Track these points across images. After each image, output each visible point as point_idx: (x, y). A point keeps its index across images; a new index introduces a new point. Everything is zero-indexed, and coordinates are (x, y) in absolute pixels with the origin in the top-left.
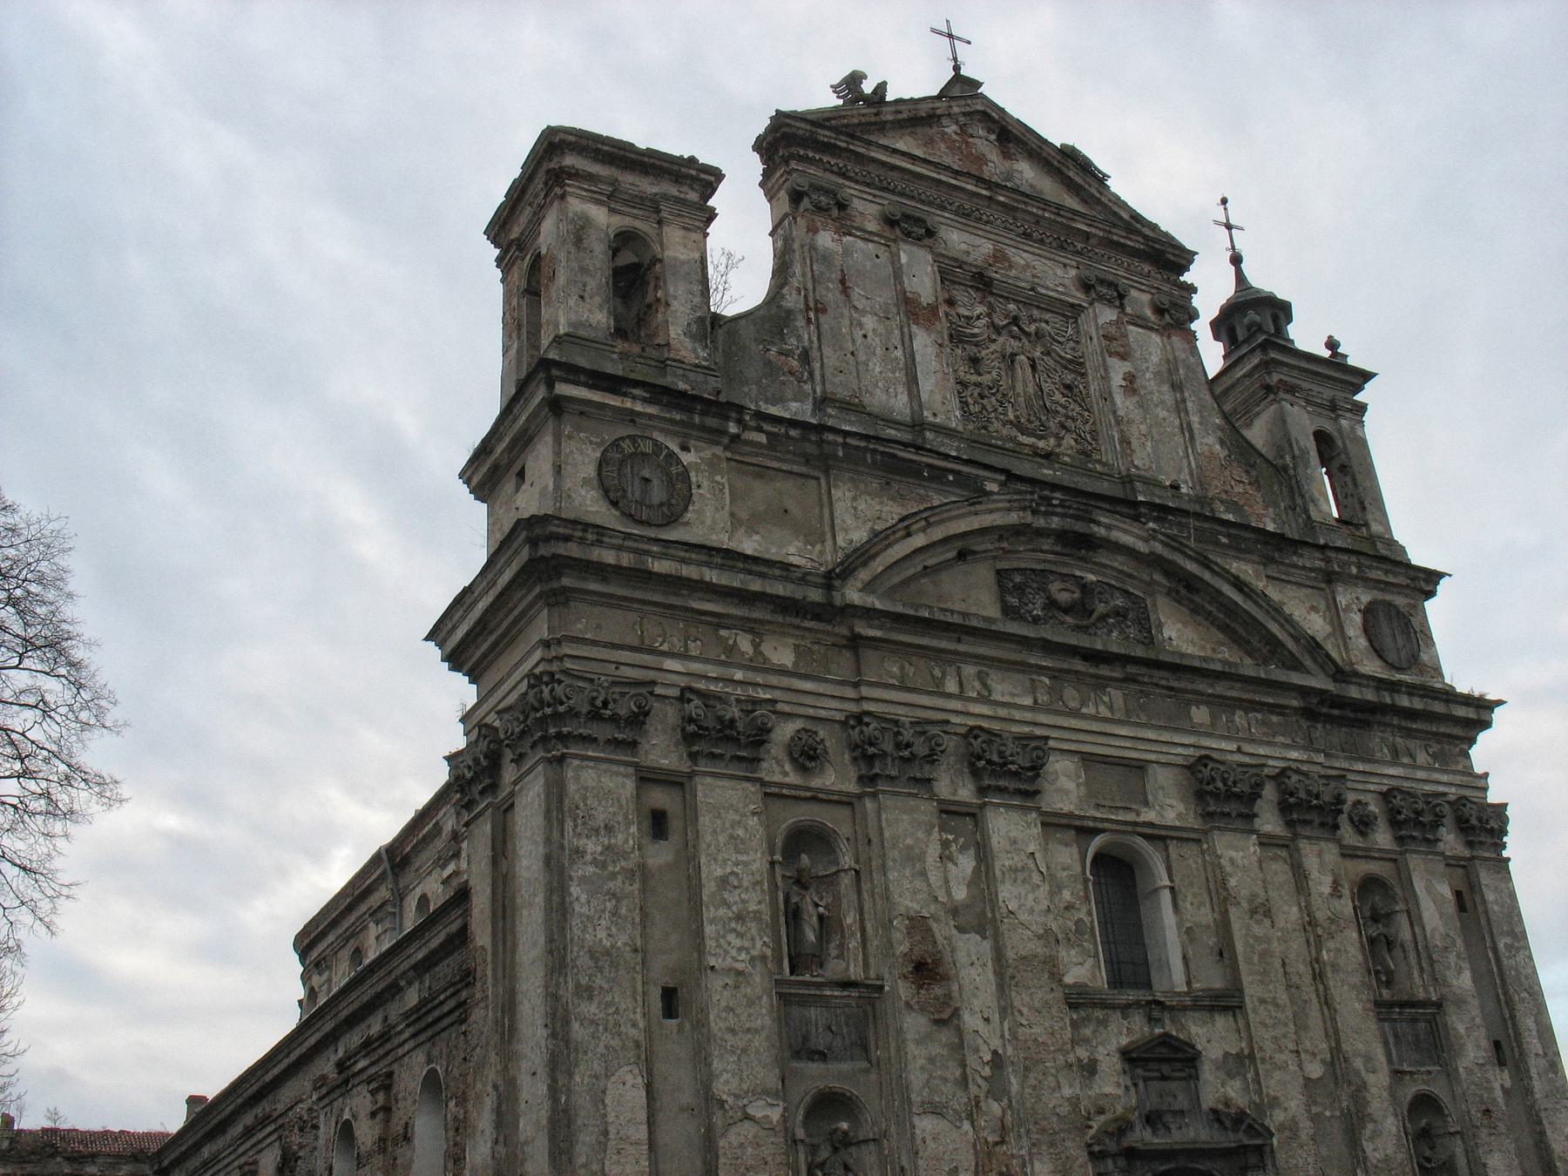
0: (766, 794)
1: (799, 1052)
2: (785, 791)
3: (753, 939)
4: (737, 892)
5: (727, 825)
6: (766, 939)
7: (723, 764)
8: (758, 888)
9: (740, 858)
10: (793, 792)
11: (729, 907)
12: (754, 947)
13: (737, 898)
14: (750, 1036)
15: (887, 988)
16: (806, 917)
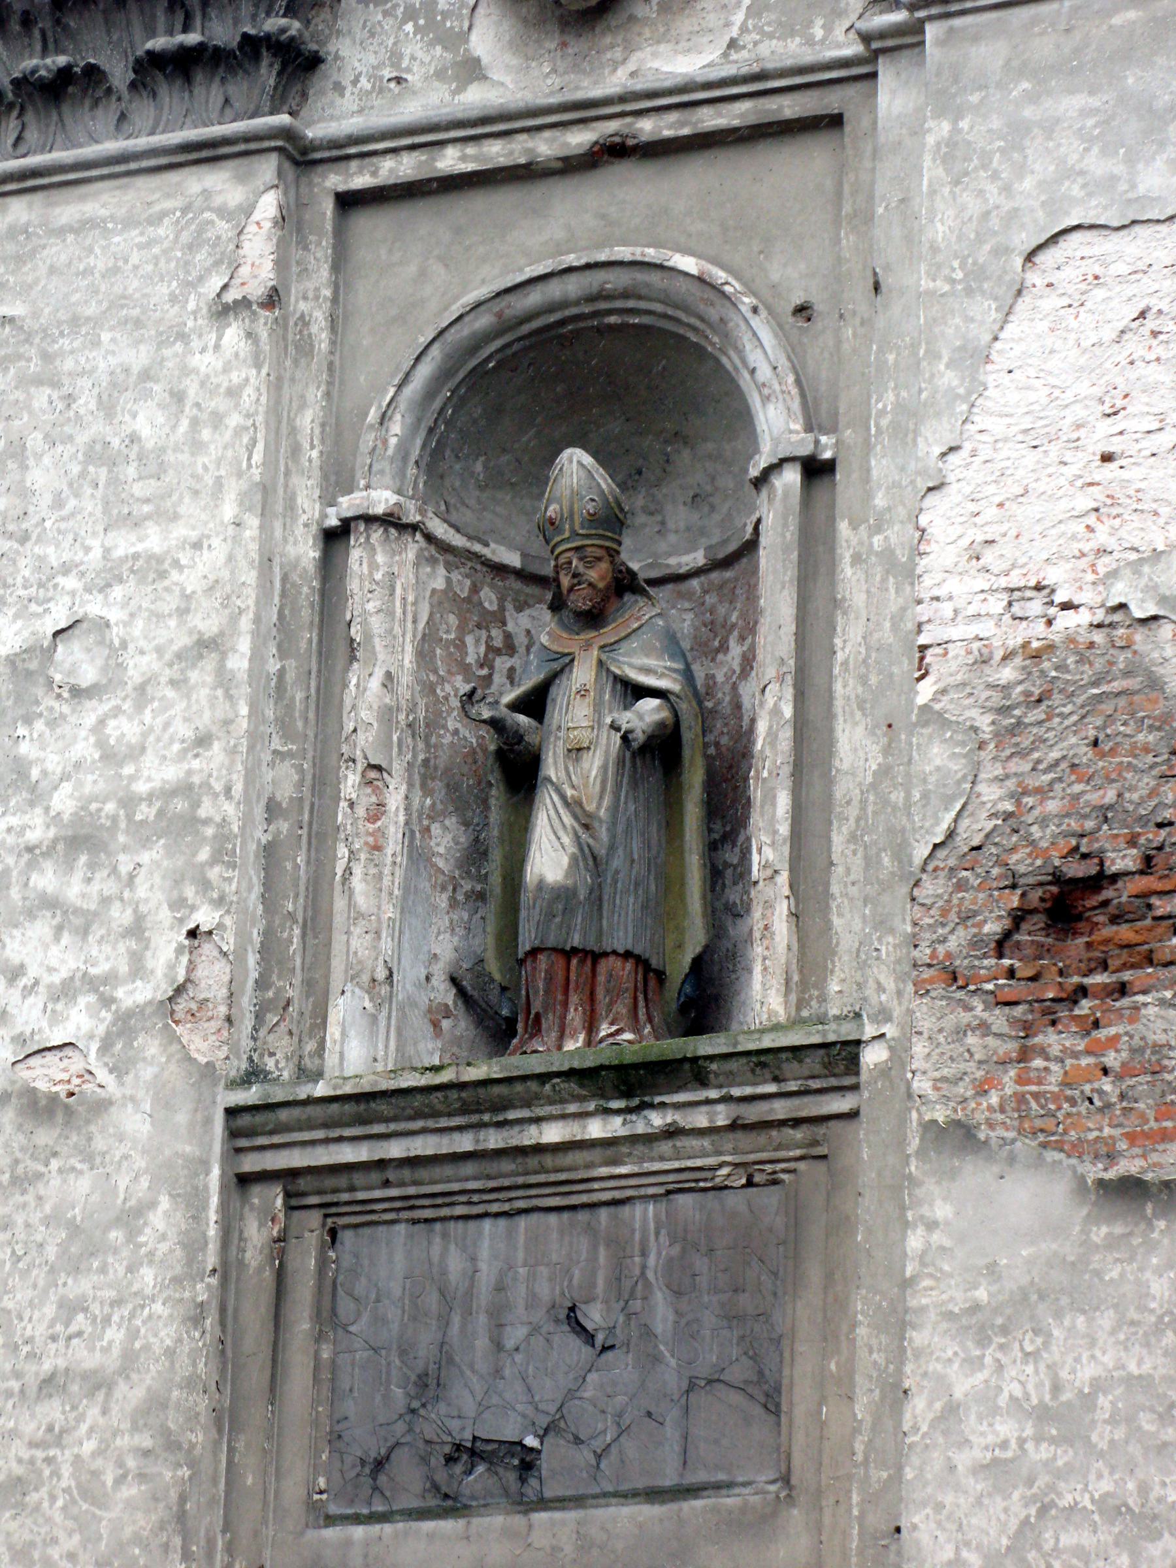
0: (348, 202)
1: (380, 1464)
2: (450, 161)
3: (137, 930)
4: (92, 712)
5: (86, 402)
6: (205, 917)
7: (105, 117)
8: (201, 676)
9: (124, 544)
10: (497, 153)
11: (36, 796)
12: (138, 969)
13: (85, 748)
14: (53, 1411)
15: (872, 1056)
16: (552, 768)
